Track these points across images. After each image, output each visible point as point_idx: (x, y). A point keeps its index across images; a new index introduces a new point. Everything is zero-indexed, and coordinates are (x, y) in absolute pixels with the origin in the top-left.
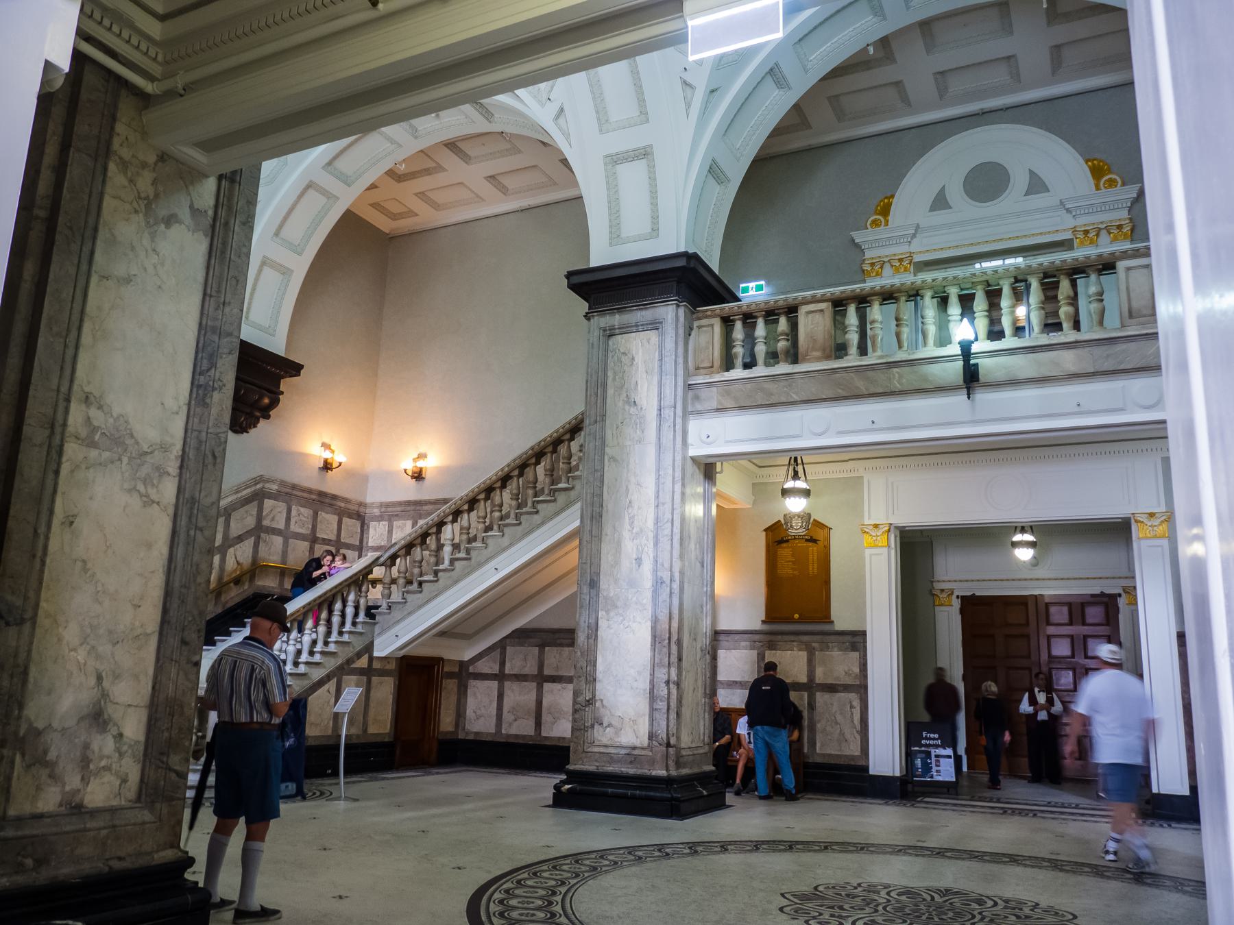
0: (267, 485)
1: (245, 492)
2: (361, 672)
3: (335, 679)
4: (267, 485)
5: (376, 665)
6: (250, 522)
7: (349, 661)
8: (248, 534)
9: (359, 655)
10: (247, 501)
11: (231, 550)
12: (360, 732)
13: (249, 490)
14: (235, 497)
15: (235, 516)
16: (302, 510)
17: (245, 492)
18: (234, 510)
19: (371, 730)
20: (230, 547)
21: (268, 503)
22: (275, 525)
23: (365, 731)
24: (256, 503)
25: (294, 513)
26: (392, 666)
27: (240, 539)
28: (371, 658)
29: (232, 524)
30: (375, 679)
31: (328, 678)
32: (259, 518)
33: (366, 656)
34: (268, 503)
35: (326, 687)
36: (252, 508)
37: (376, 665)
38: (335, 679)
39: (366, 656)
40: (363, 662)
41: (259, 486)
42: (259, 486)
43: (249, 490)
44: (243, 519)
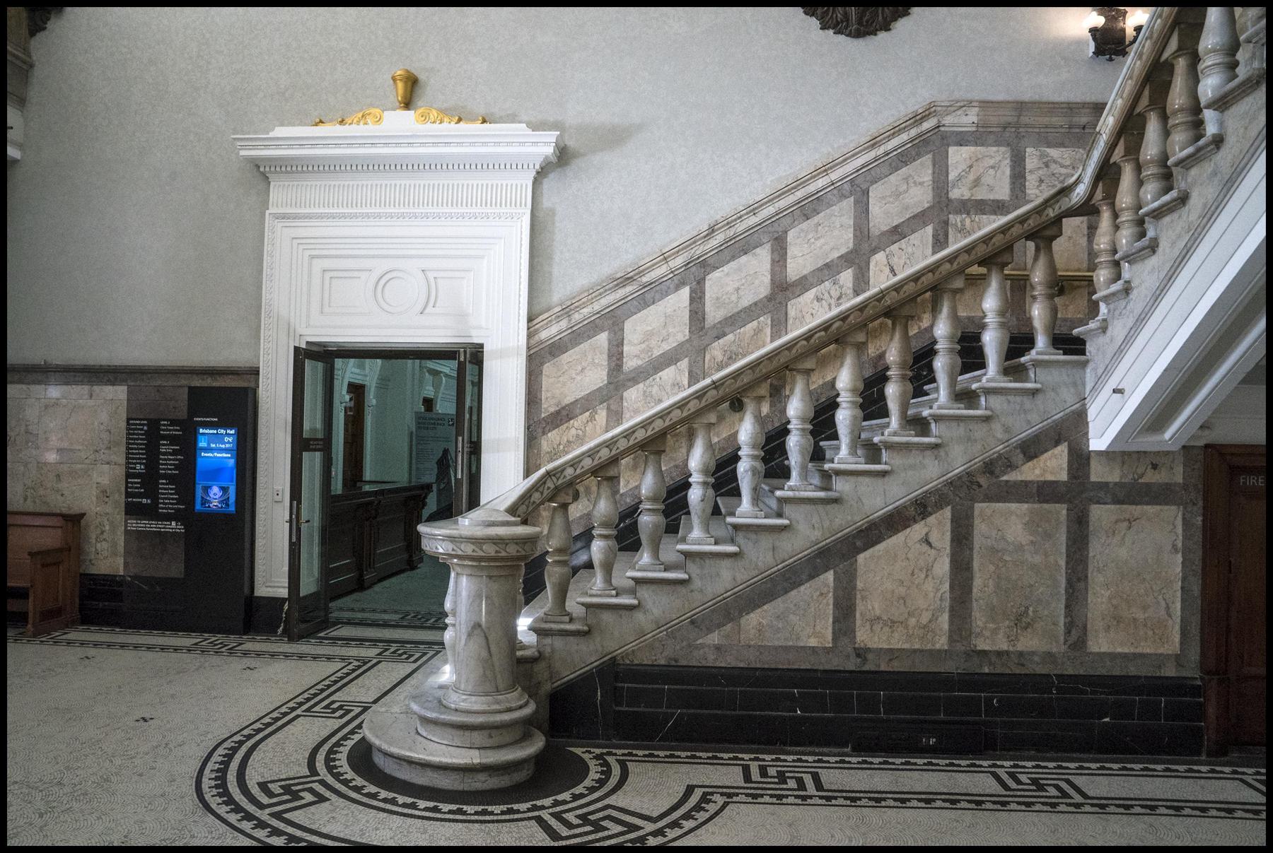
0: (948, 120)
1: (895, 142)
2: (1045, 492)
3: (947, 512)
4: (948, 120)
5: (1098, 473)
6: (920, 196)
7: (990, 467)
8: (919, 219)
9: (1031, 449)
10: (903, 158)
11: (880, 257)
12: (1058, 648)
13: (904, 137)
14: (872, 154)
15: (876, 192)
16: (1054, 153)
17: (895, 142)
18: (874, 182)
19: (1101, 643)
20: (874, 251)
21: (958, 157)
22: (981, 194)
23: (1079, 644)
24: (927, 160)
25: (1032, 161)
26: (1178, 475)
27: (897, 233)
28: (1080, 458)
29: (875, 209)
30: (1101, 514)
31: (922, 507)
32: (941, 184)
33: (1062, 450)
34: (958, 157)
35: (918, 530)
36: (922, 170)
37: (1098, 473)
38: (947, 512)
39: (1062, 450)
40: (1053, 465)
41: (927, 125)
42: (927, 125)
43: (904, 137)
44: (897, 195)
